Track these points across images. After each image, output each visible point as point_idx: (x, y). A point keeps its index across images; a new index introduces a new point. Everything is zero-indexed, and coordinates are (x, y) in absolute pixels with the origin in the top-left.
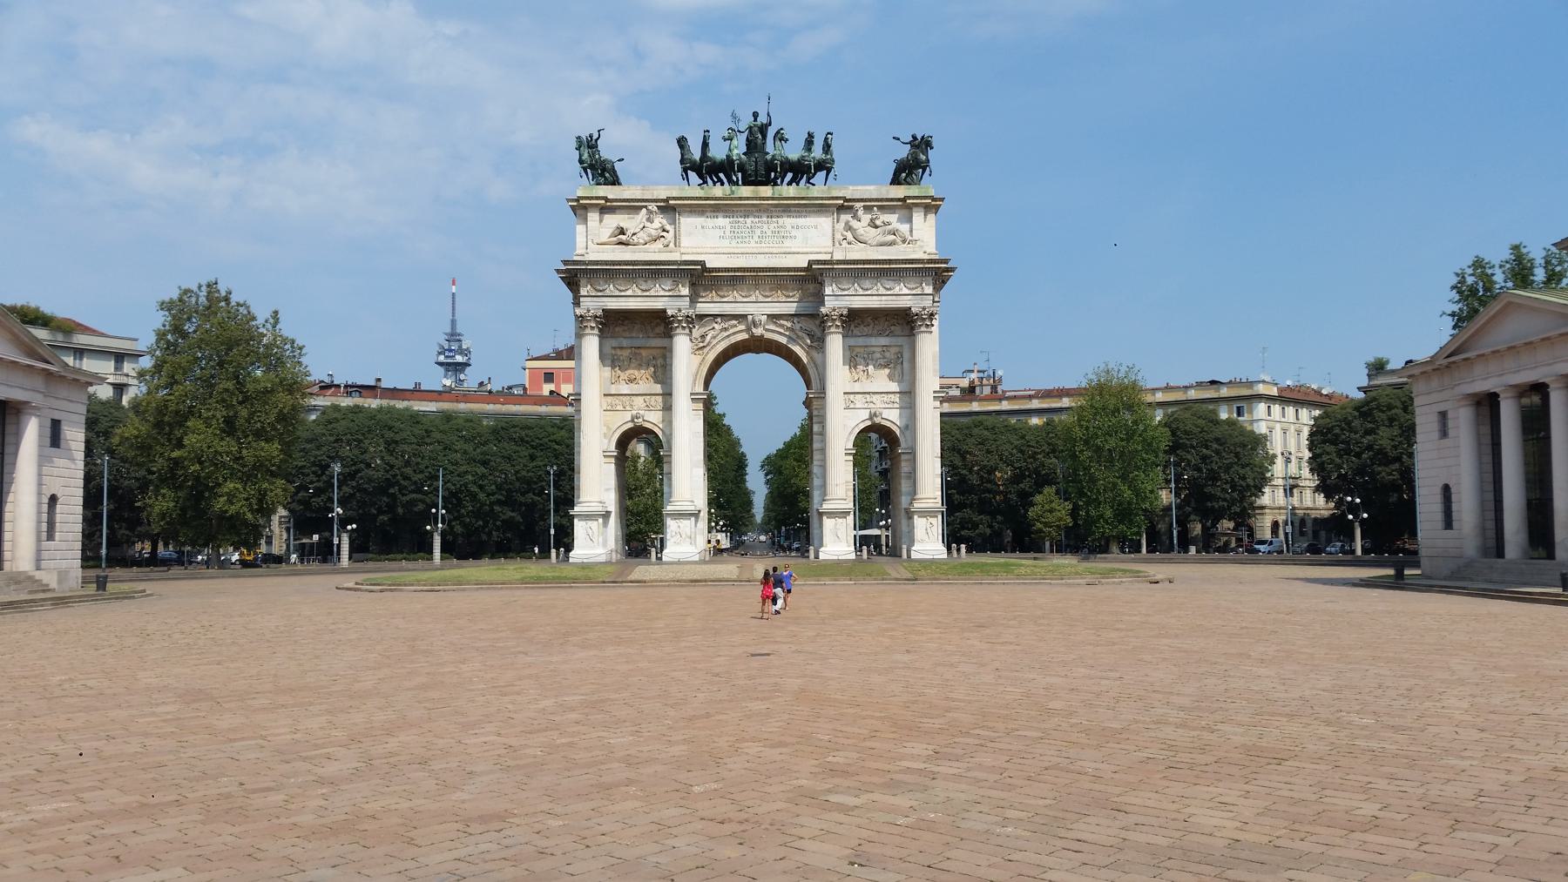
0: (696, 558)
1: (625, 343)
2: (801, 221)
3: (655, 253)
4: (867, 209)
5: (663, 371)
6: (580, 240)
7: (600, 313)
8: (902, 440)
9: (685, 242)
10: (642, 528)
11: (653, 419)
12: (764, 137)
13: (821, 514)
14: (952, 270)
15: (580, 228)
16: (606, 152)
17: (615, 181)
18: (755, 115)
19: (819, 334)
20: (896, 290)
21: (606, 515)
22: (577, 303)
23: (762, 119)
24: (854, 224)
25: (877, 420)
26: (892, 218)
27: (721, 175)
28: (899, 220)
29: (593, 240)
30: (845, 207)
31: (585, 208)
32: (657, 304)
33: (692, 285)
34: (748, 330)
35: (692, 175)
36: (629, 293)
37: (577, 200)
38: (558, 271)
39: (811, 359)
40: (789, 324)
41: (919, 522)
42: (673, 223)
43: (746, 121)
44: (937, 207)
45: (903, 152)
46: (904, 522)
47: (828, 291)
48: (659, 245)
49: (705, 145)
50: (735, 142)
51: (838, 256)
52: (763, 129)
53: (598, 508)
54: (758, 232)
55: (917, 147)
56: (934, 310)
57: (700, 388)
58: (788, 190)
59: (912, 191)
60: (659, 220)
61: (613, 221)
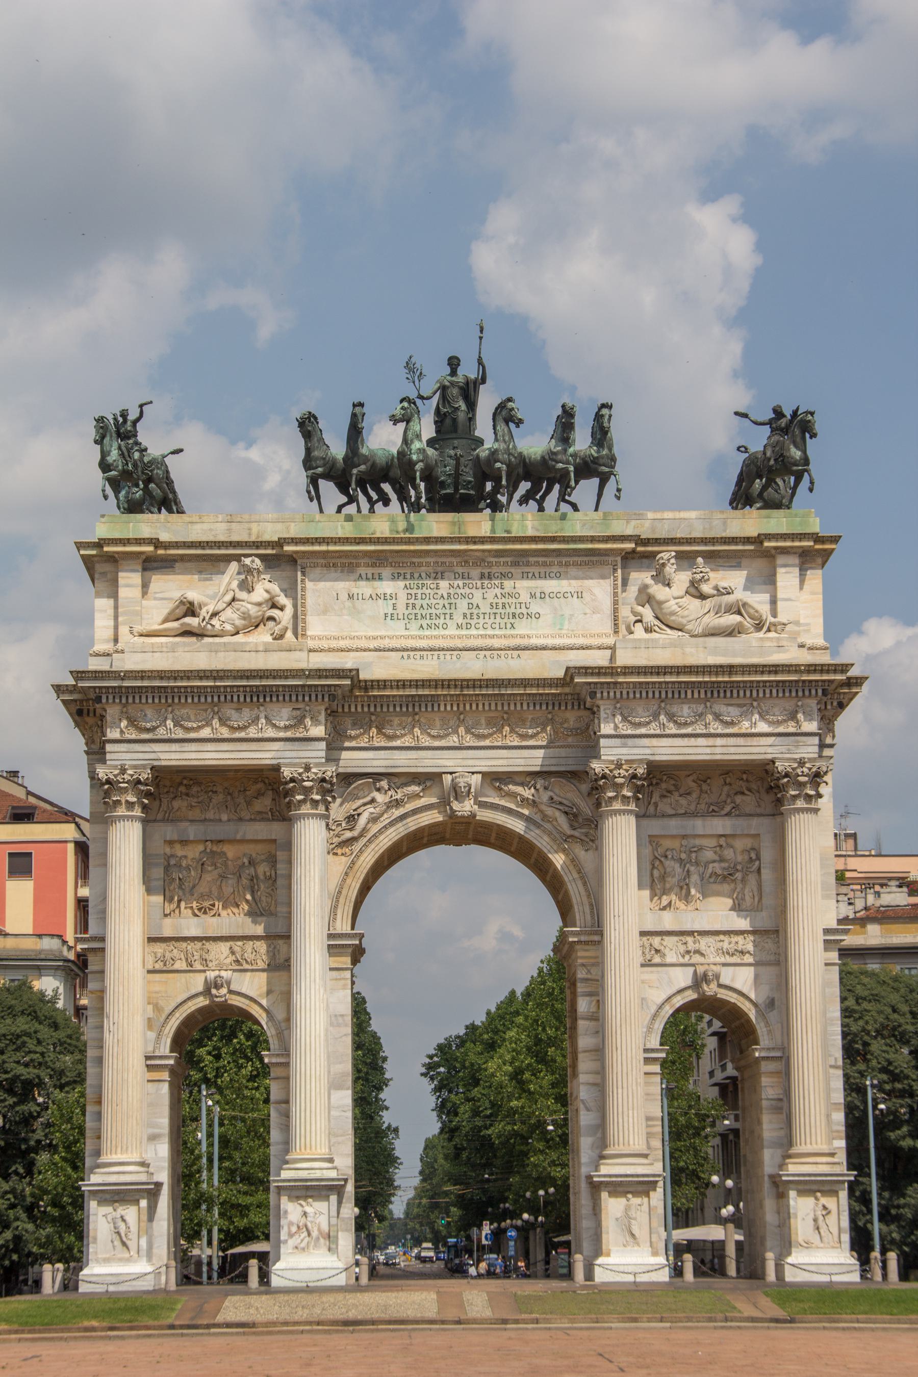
0: (341, 1280)
1: (192, 831)
2: (551, 585)
3: (256, 652)
4: (685, 559)
5: (268, 891)
6: (103, 624)
7: (145, 775)
8: (761, 1030)
9: (315, 626)
10: (224, 1218)
11: (250, 988)
12: (472, 405)
13: (595, 1188)
14: (858, 682)
15: (103, 605)
16: (153, 441)
17: (167, 502)
18: (454, 363)
19: (586, 808)
20: (745, 726)
21: (153, 1192)
22: (96, 752)
23: (469, 371)
24: (659, 592)
25: (710, 989)
26: (734, 579)
27: (386, 487)
28: (749, 586)
29: (134, 629)
30: (639, 554)
31: (113, 559)
32: (264, 756)
33: (332, 713)
34: (444, 802)
35: (327, 488)
36: (206, 733)
37: (99, 544)
38: (59, 689)
39: (574, 861)
40: (528, 793)
41: (802, 1208)
42: (291, 590)
43: (435, 373)
44: (829, 553)
45: (759, 440)
46: (769, 1204)
47: (606, 728)
48: (263, 636)
49: (355, 432)
50: (414, 426)
51: (625, 658)
52: (469, 392)
53: (133, 1175)
54: (463, 605)
55: (785, 431)
56: (822, 765)
57: (343, 926)
58: (522, 520)
59: (775, 522)
60: (265, 587)
61: (172, 587)
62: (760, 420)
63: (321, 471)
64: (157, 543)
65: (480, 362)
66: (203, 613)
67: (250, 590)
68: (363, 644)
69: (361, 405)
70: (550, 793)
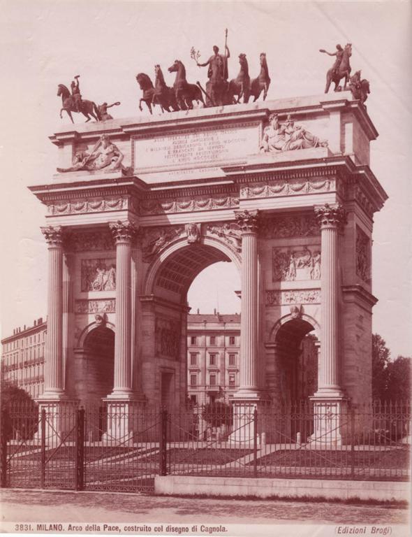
16: (86, 95)
18: (216, 49)
23: (222, 52)
62: (332, 53)
63: (149, 100)
64: (75, 133)
65: (226, 47)
66: (84, 160)
67: (105, 148)
68: (153, 169)
69: (158, 66)
70: (230, 230)
